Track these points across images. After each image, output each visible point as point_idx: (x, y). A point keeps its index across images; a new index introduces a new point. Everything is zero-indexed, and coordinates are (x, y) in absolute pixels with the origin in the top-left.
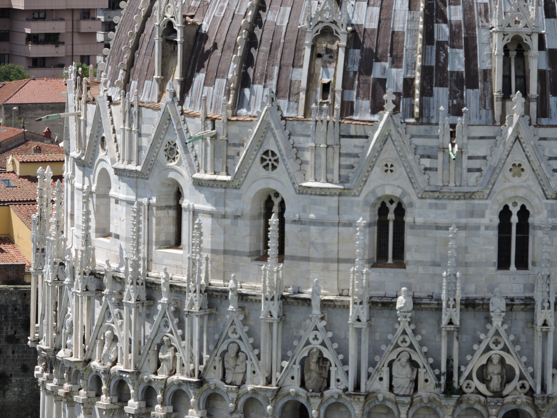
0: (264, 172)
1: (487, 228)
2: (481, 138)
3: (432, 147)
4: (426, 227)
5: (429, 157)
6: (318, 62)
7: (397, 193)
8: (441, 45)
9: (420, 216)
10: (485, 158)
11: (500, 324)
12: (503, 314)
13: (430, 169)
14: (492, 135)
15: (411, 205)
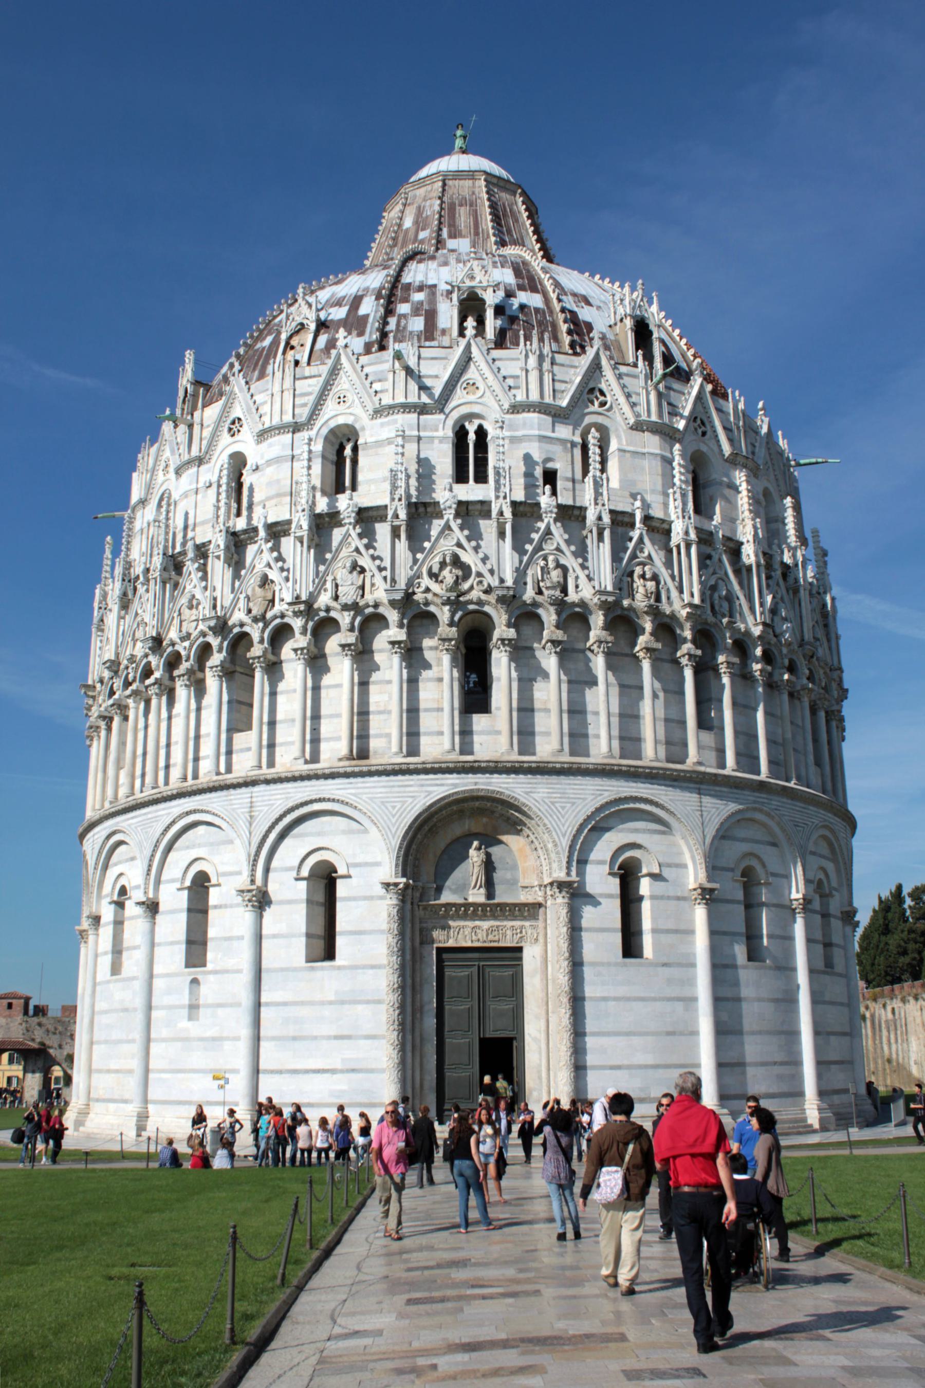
0: (231, 440)
1: (441, 442)
2: (432, 359)
3: (382, 371)
4: (379, 444)
5: (380, 381)
6: (292, 352)
7: (349, 420)
8: (404, 316)
9: (372, 436)
10: (437, 377)
11: (451, 517)
12: (454, 506)
13: (382, 391)
14: (443, 356)
15: (363, 429)
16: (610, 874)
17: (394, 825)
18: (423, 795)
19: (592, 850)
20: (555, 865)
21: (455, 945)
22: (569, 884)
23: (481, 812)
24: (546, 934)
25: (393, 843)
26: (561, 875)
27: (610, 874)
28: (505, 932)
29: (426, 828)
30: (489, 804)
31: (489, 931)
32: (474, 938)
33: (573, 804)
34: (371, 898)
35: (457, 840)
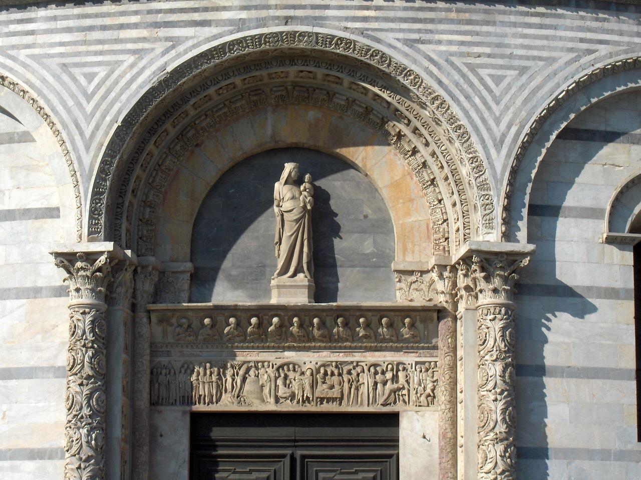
16: (610, 241)
17: (89, 118)
18: (160, 47)
19: (571, 183)
20: (477, 218)
21: (235, 408)
22: (511, 259)
23: (302, 94)
24: (454, 382)
25: (87, 160)
26: (491, 238)
27: (610, 241)
28: (359, 378)
29: (171, 129)
30: (320, 72)
31: (319, 374)
32: (282, 391)
33: (523, 70)
34: (35, 292)
35: (248, 161)
